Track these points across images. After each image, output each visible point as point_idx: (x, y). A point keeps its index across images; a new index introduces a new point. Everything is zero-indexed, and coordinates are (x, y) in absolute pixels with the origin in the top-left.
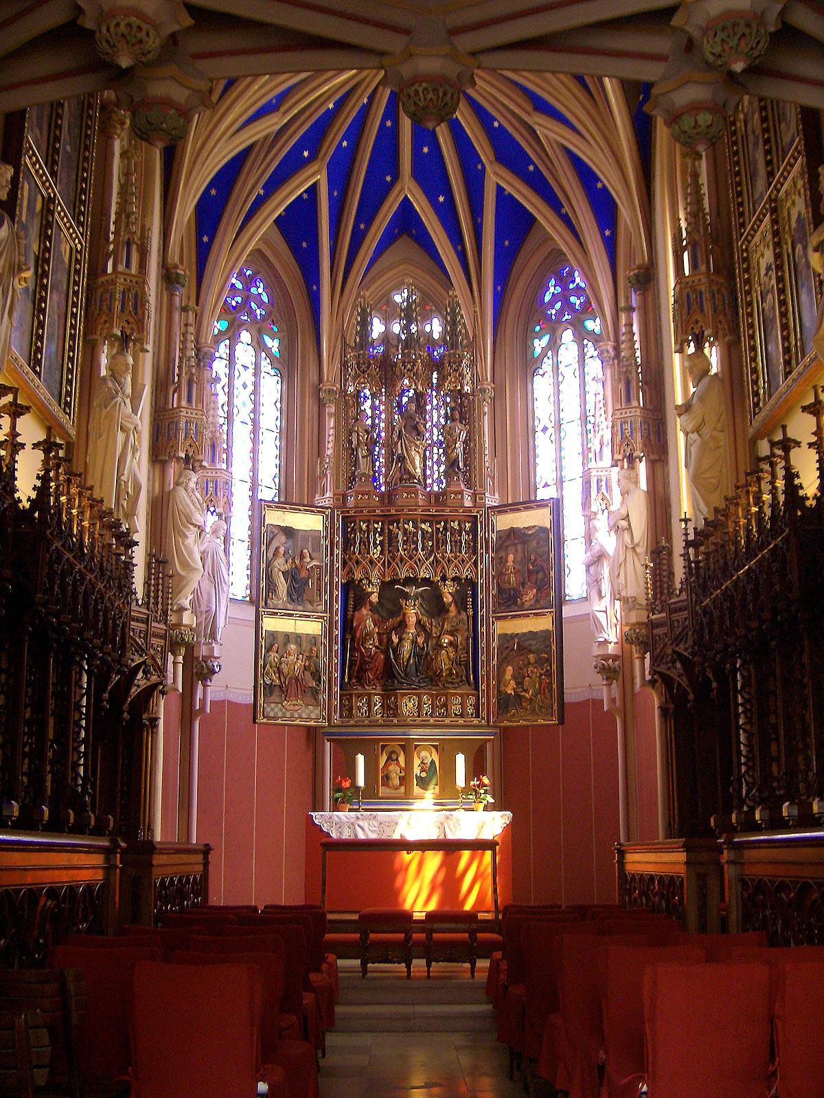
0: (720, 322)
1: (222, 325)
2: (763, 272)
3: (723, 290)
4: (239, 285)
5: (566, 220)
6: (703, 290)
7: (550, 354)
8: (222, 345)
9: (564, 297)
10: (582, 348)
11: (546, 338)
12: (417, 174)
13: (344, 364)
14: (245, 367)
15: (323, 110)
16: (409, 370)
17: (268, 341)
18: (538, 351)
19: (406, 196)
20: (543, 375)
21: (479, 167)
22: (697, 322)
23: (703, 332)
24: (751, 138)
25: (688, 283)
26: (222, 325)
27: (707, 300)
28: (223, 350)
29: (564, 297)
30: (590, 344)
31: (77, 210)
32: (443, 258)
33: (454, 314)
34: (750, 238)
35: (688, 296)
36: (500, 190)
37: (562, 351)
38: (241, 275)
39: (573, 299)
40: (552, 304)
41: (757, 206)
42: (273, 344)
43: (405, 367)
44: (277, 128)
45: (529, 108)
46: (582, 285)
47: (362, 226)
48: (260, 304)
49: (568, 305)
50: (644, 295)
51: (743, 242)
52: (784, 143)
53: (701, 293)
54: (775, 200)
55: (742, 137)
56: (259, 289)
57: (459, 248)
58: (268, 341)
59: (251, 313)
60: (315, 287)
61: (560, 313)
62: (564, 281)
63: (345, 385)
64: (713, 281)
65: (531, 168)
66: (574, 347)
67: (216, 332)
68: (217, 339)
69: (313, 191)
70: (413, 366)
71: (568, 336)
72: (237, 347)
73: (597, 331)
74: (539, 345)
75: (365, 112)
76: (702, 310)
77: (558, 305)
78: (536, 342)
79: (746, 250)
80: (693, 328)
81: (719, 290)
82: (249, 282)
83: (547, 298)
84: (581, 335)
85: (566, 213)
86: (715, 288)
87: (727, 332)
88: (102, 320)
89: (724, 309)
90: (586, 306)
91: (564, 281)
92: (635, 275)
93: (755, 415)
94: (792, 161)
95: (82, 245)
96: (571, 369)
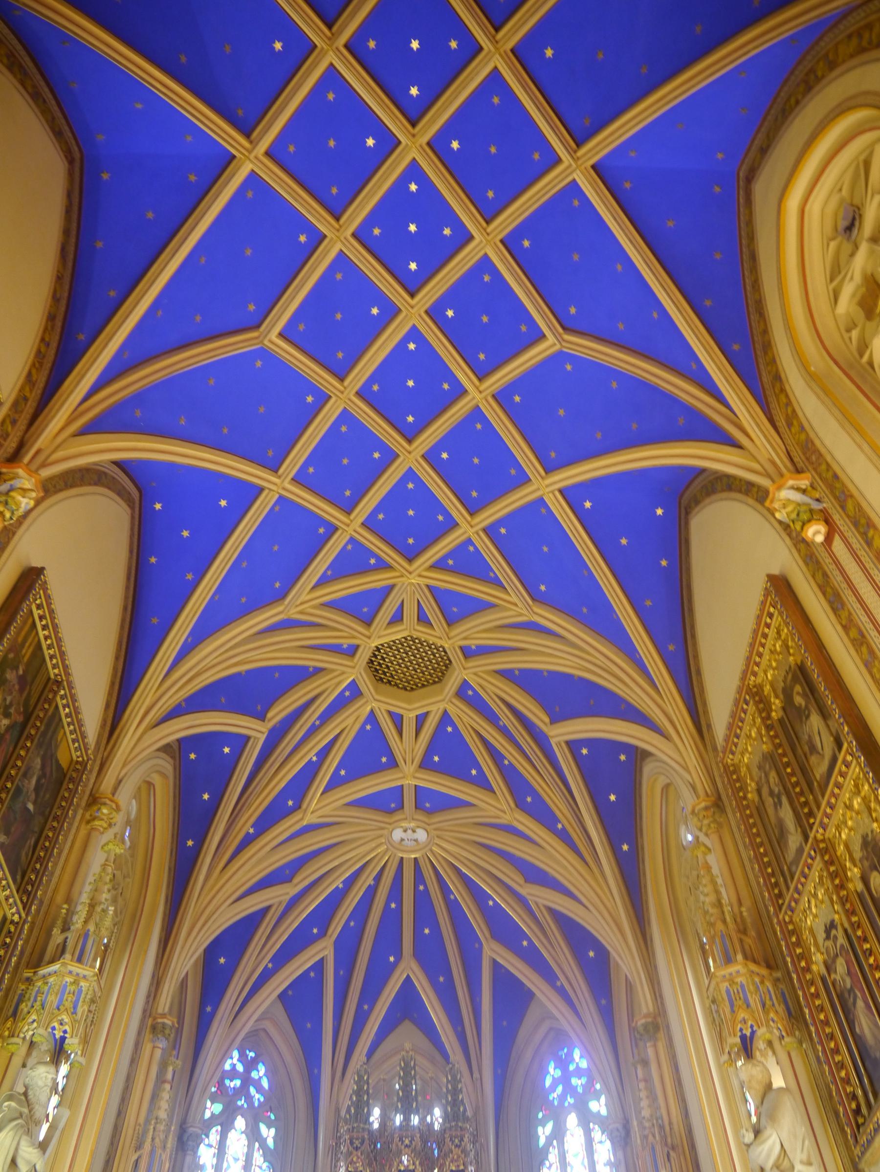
0: (773, 1021)
1: (217, 1108)
2: (821, 935)
3: (768, 984)
4: (240, 1068)
5: (562, 992)
6: (744, 982)
7: (555, 1142)
8: (214, 1130)
9: (565, 1079)
10: (588, 1133)
11: (550, 1126)
12: (419, 955)
13: (338, 1139)
14: (236, 1160)
15: (334, 887)
16: (406, 1146)
17: (263, 1128)
18: (542, 1141)
19: (408, 976)
20: (549, 1168)
21: (477, 945)
22: (744, 1021)
23: (753, 1033)
24: (769, 801)
25: (724, 976)
26: (217, 1108)
27: (751, 993)
28: (214, 1136)
29: (565, 1079)
30: (596, 1127)
31: (26, 878)
32: (443, 1039)
33: (455, 1092)
34: (793, 904)
35: (728, 991)
36: (495, 965)
37: (568, 1138)
38: (243, 1057)
39: (575, 1081)
40: (553, 1088)
41: (794, 869)
42: (268, 1133)
43: (403, 1142)
44: (288, 898)
45: (521, 880)
46: (584, 1064)
47: (366, 1007)
48: (260, 1089)
49: (569, 1089)
50: (655, 1046)
51: (786, 913)
52: (818, 777)
53: (742, 986)
54: (823, 841)
55: (757, 809)
56: (260, 1072)
57: (459, 1029)
58: (263, 1128)
59: (249, 1098)
60: (316, 1071)
61: (562, 1098)
62: (563, 1064)
63: (336, 1166)
64: (753, 972)
65: (525, 943)
66: (580, 1132)
67: (208, 1115)
68: (207, 1126)
69: (319, 966)
70: (411, 1142)
71: (572, 1120)
72: (230, 1135)
73: (604, 1112)
74: (544, 1132)
75: (371, 892)
76: (748, 1006)
77: (560, 1089)
78: (540, 1130)
79: (791, 922)
80: (741, 1030)
81: (762, 982)
82: (250, 1065)
83: (548, 1082)
84: (586, 1119)
85: (562, 985)
86: (757, 980)
87: (784, 1034)
88: (31, 1020)
89: (773, 1005)
90: (589, 1087)
91: (563, 1064)
92: (643, 1025)
93: (858, 1127)
94: (840, 779)
95: (20, 917)
96: (581, 1156)
